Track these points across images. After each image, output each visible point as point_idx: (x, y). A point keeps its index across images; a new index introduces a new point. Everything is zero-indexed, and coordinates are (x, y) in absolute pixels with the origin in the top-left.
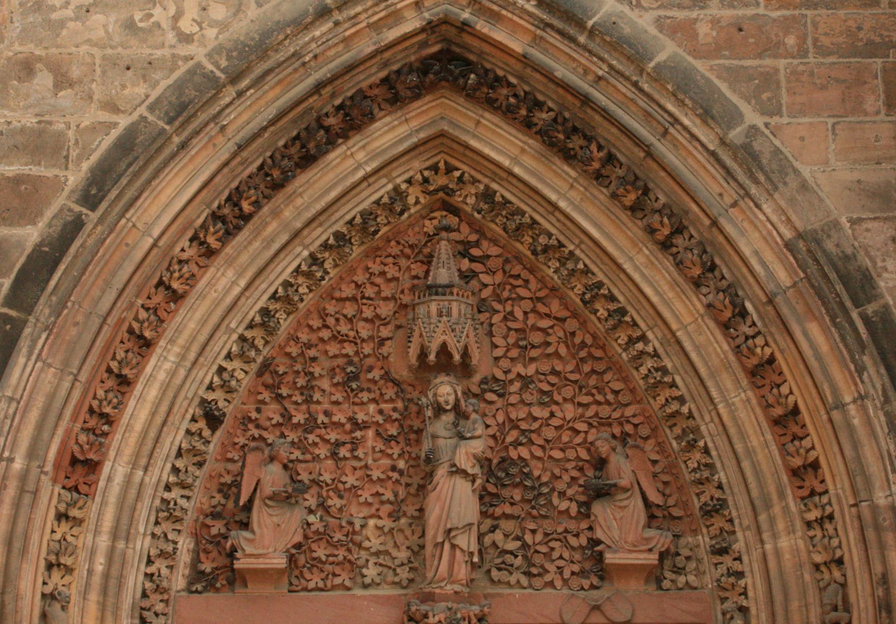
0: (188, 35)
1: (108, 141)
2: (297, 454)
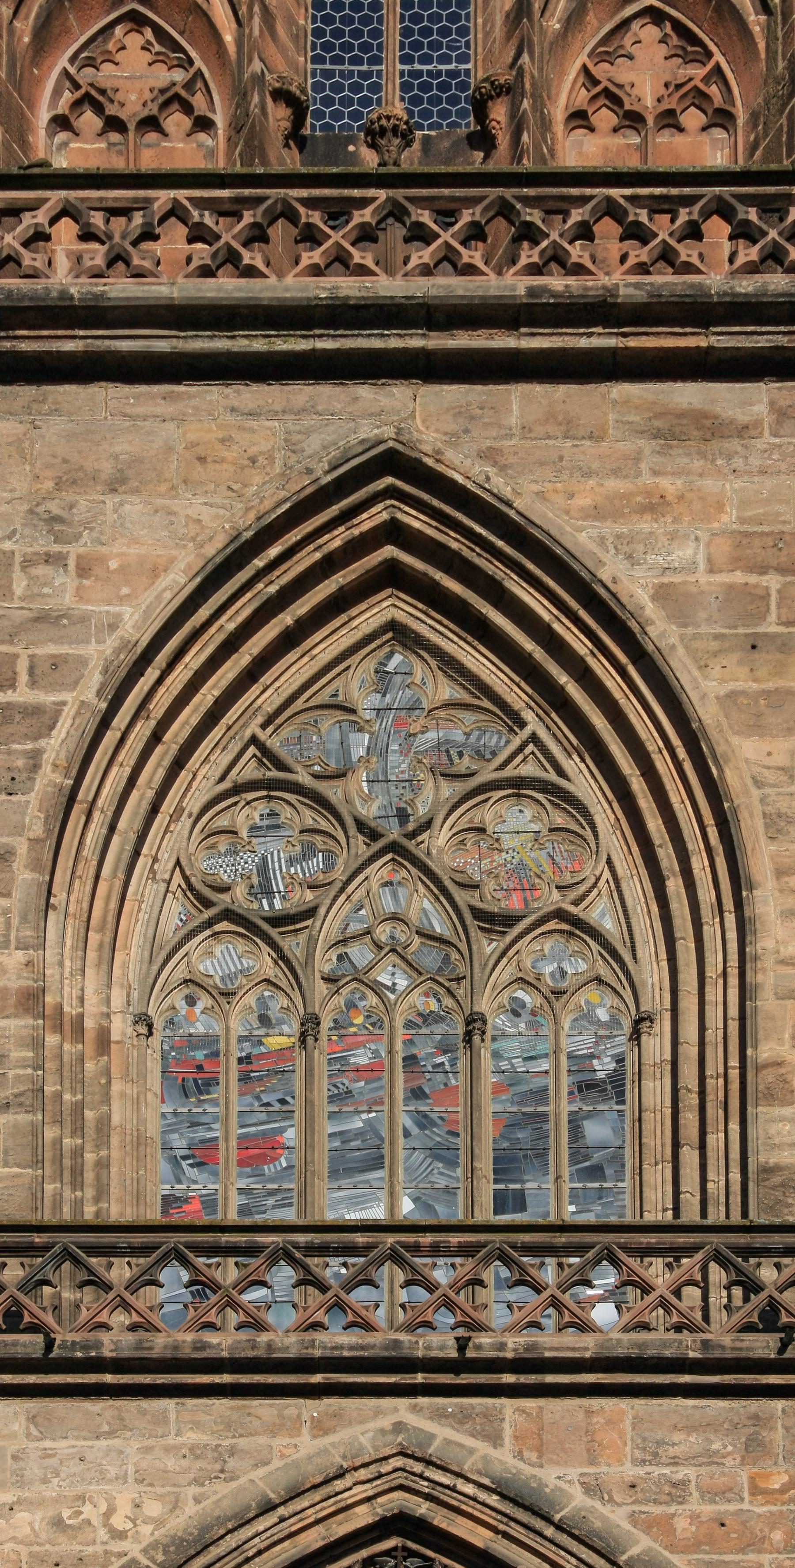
0: (121, 1532)
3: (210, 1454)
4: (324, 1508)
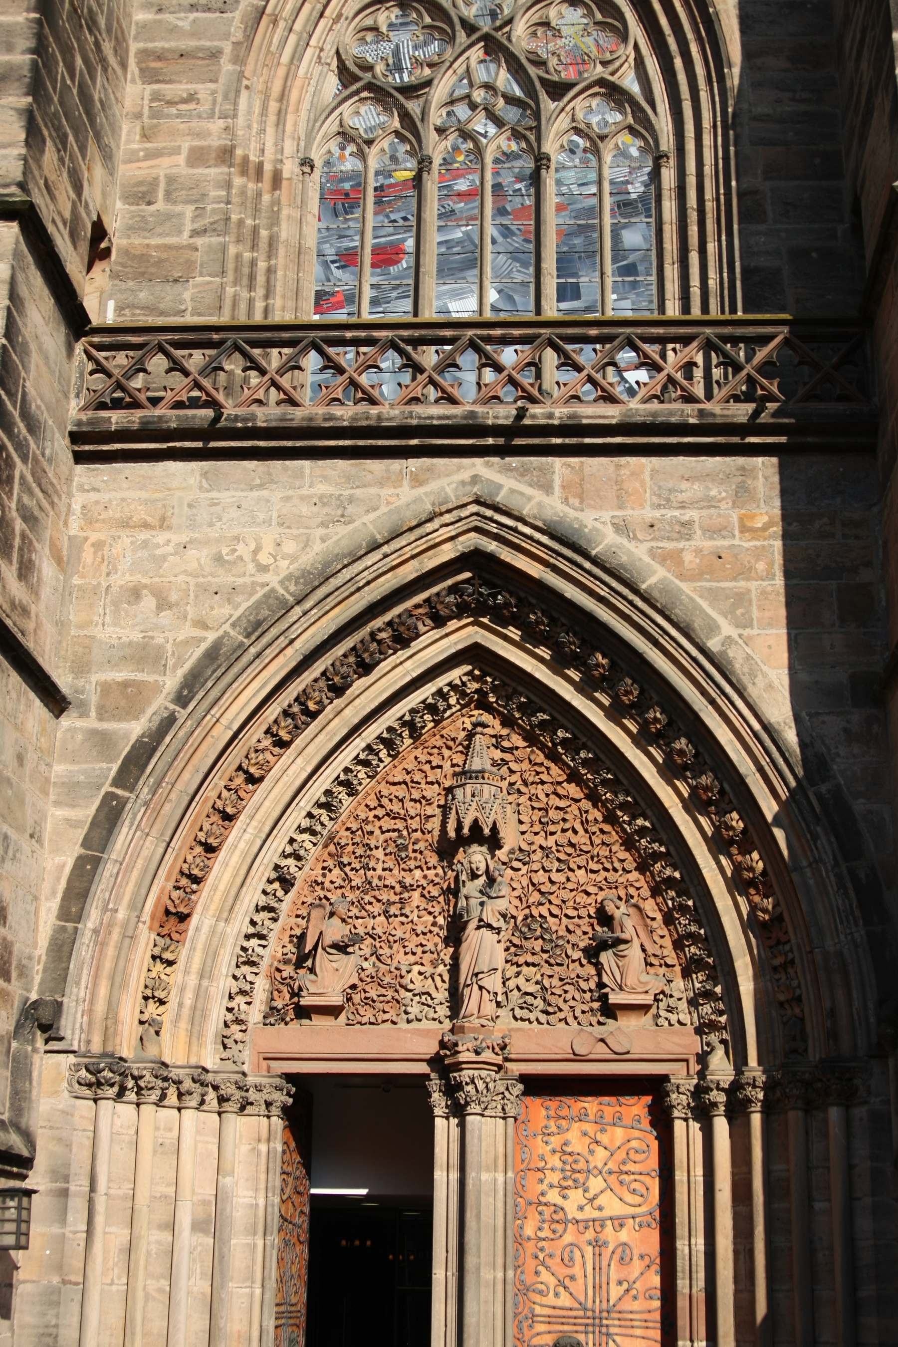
1: (199, 652)
2: (355, 911)
3: (334, 502)
4: (418, 546)
